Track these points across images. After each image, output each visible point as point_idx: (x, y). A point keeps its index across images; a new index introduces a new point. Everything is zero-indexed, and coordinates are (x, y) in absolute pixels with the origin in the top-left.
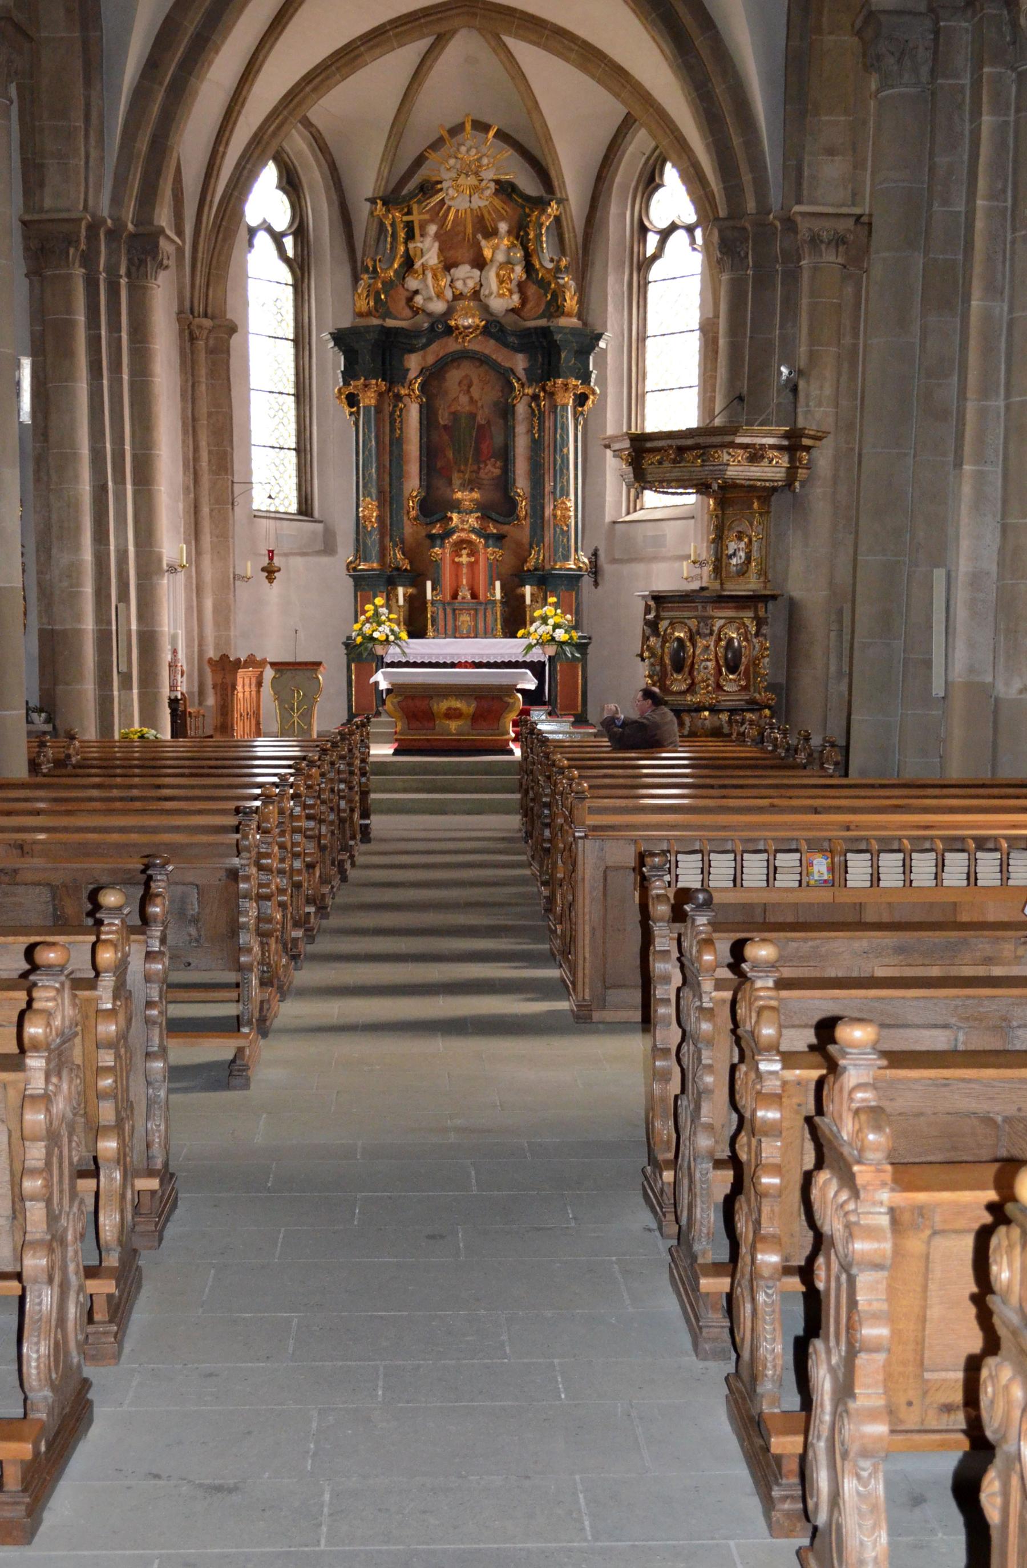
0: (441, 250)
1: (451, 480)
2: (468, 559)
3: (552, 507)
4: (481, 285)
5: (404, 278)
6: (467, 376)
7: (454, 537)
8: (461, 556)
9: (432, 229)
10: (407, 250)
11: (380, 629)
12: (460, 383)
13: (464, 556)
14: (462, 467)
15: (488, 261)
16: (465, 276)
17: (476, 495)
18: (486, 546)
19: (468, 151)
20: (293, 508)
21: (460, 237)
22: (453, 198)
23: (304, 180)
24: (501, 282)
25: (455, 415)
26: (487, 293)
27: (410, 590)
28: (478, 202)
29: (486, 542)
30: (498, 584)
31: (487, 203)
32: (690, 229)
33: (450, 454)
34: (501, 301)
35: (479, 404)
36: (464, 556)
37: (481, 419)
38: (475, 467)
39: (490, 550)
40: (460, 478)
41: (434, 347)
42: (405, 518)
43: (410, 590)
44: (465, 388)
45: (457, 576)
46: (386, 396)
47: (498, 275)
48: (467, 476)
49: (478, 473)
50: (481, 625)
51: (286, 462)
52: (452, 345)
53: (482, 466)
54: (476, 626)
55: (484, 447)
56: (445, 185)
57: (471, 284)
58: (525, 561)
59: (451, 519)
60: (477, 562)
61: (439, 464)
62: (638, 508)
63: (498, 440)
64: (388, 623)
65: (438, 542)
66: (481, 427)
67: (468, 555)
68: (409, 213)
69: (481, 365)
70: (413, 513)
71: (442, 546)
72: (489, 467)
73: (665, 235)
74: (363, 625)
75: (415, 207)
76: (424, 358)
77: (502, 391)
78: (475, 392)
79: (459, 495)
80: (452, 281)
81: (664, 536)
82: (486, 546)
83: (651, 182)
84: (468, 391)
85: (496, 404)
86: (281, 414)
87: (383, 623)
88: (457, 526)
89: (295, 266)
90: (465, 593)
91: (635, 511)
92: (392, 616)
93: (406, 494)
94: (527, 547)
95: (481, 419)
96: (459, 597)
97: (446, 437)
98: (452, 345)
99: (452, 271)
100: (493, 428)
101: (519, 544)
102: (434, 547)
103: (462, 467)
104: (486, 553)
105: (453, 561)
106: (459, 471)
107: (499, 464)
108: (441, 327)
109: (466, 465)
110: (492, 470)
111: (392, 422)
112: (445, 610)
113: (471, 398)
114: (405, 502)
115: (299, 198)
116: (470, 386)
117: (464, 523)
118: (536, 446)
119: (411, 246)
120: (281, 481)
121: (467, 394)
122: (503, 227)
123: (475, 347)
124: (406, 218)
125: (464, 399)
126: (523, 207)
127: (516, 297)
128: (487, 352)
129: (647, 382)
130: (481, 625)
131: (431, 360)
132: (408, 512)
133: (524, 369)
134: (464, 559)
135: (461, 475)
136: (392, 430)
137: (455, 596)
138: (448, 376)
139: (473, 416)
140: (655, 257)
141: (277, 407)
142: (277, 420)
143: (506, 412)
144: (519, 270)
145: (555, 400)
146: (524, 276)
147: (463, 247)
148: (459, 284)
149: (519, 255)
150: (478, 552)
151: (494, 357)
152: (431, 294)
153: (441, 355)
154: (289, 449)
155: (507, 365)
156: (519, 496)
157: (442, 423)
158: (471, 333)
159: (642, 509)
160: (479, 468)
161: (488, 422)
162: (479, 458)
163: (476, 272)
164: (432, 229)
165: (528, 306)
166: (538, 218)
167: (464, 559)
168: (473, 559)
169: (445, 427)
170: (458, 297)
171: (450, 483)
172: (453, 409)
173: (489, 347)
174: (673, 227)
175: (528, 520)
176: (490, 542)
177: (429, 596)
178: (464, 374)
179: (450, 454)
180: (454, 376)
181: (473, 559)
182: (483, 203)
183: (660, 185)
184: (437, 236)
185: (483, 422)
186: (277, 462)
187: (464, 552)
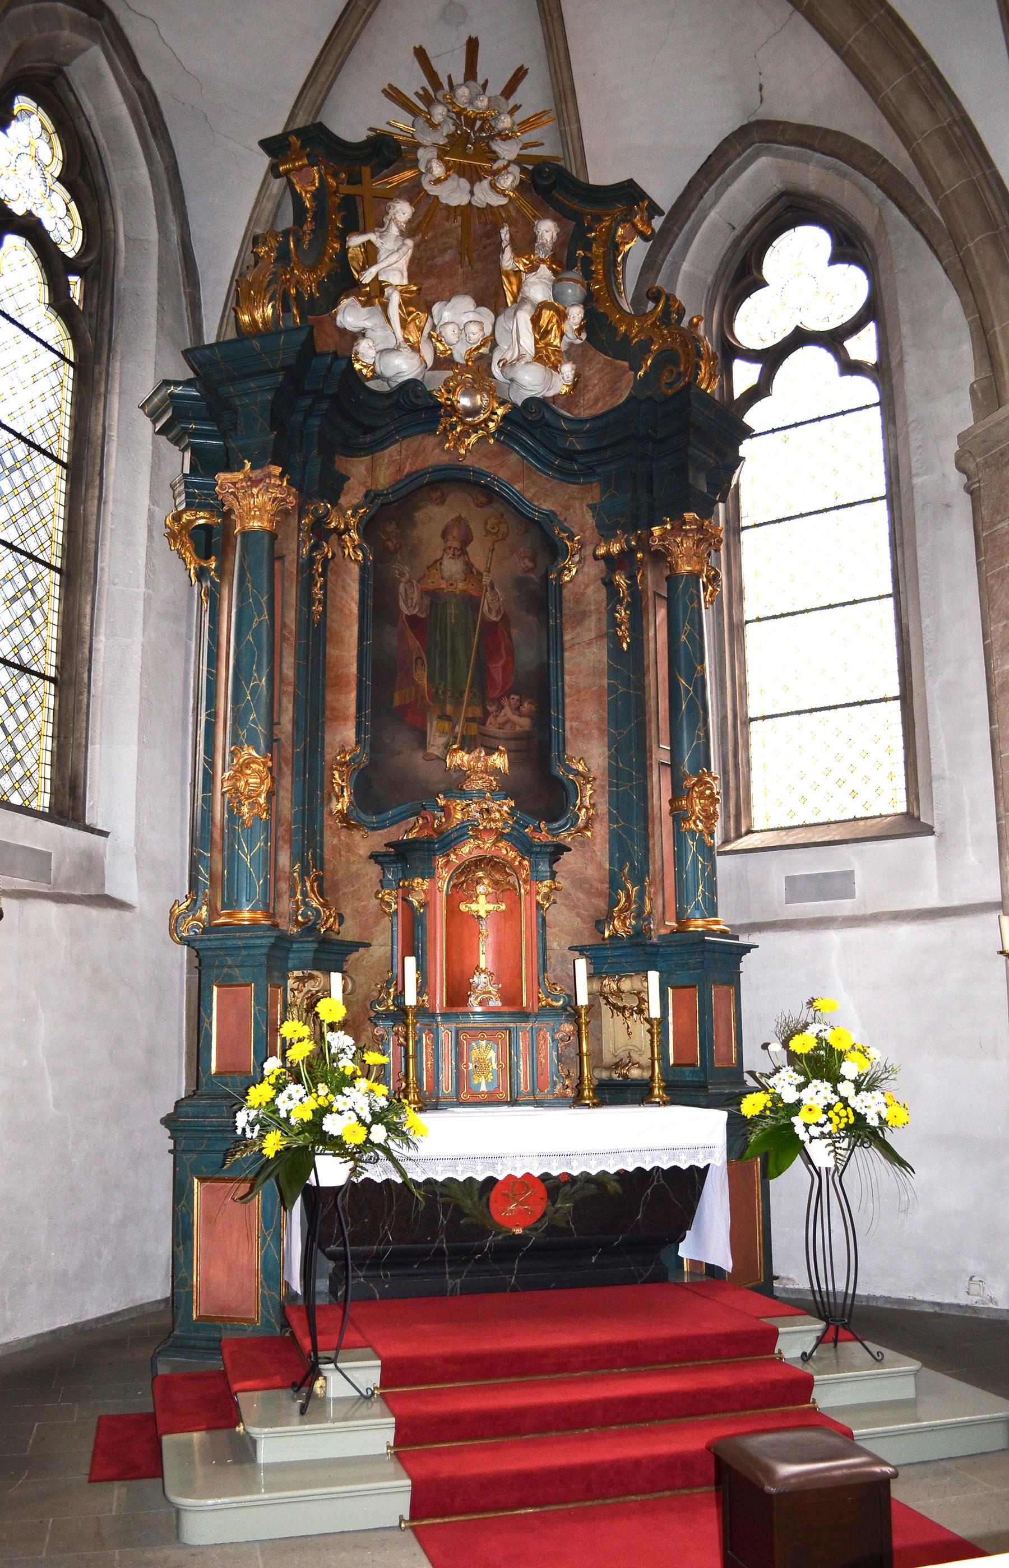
0: (416, 269)
1: (424, 734)
2: (491, 907)
3: (667, 795)
4: (494, 345)
5: (336, 304)
6: (459, 520)
7: (466, 850)
8: (472, 898)
9: (402, 211)
10: (345, 250)
11: (340, 1103)
12: (444, 535)
13: (482, 899)
14: (449, 709)
15: (509, 299)
16: (460, 322)
17: (500, 761)
19: (471, 102)
20: (43, 802)
21: (448, 257)
22: (438, 181)
23: (115, 177)
24: (542, 334)
25: (435, 598)
26: (508, 357)
28: (485, 196)
31: (504, 201)
32: (833, 340)
33: (422, 678)
34: (532, 381)
35: (486, 580)
36: (482, 899)
37: (489, 609)
38: (478, 712)
40: (443, 733)
41: (392, 451)
44: (456, 544)
46: (294, 521)
47: (535, 320)
48: (458, 729)
49: (483, 723)
51: (33, 702)
52: (429, 452)
53: (492, 708)
55: (497, 669)
56: (421, 153)
57: (475, 335)
58: (610, 918)
61: (397, 700)
62: (743, 830)
63: (527, 657)
64: (362, 1083)
66: (489, 629)
68: (355, 180)
69: (490, 502)
70: (341, 805)
72: (507, 711)
73: (771, 359)
74: (279, 1088)
75: (366, 171)
76: (372, 470)
77: (532, 559)
78: (477, 553)
80: (434, 327)
81: (849, 875)
83: (743, 277)
84: (462, 552)
85: (521, 583)
86: (28, 598)
87: (350, 1081)
89: (84, 326)
91: (739, 836)
92: (373, 1058)
93: (331, 753)
95: (489, 609)
97: (414, 643)
98: (429, 452)
99: (436, 309)
100: (514, 632)
103: (449, 709)
106: (443, 717)
107: (526, 706)
108: (413, 407)
109: (458, 704)
110: (514, 717)
111: (307, 583)
113: (469, 566)
115: (101, 212)
116: (466, 540)
118: (628, 665)
119: (355, 241)
120: (19, 742)
121: (455, 558)
122: (547, 230)
123: (482, 465)
124: (346, 189)
125: (452, 567)
126: (577, 217)
127: (568, 370)
128: (503, 474)
129: (746, 605)
130: (523, 1070)
131: (384, 479)
133: (592, 507)
135: (446, 725)
136: (307, 599)
138: (419, 515)
139: (472, 603)
140: (760, 391)
141: (21, 583)
142: (18, 608)
143: (543, 600)
144: (576, 314)
145: (672, 567)
146: (584, 336)
147: (461, 259)
148: (450, 333)
149: (573, 291)
151: (517, 487)
152: (385, 348)
153: (407, 469)
154: (42, 676)
155: (546, 506)
156: (577, 773)
157: (406, 611)
158: (475, 428)
159: (750, 832)
160: (486, 714)
161: (505, 618)
162: (485, 691)
163: (486, 315)
164: (402, 211)
165: (590, 396)
166: (612, 232)
167: (482, 906)
169: (412, 620)
170: (443, 362)
171: (422, 742)
172: (430, 584)
173: (509, 470)
174: (800, 338)
178: (453, 516)
179: (422, 678)
180: (434, 518)
182: (498, 201)
183: (761, 283)
184: (409, 231)
185: (493, 617)
186: (13, 697)
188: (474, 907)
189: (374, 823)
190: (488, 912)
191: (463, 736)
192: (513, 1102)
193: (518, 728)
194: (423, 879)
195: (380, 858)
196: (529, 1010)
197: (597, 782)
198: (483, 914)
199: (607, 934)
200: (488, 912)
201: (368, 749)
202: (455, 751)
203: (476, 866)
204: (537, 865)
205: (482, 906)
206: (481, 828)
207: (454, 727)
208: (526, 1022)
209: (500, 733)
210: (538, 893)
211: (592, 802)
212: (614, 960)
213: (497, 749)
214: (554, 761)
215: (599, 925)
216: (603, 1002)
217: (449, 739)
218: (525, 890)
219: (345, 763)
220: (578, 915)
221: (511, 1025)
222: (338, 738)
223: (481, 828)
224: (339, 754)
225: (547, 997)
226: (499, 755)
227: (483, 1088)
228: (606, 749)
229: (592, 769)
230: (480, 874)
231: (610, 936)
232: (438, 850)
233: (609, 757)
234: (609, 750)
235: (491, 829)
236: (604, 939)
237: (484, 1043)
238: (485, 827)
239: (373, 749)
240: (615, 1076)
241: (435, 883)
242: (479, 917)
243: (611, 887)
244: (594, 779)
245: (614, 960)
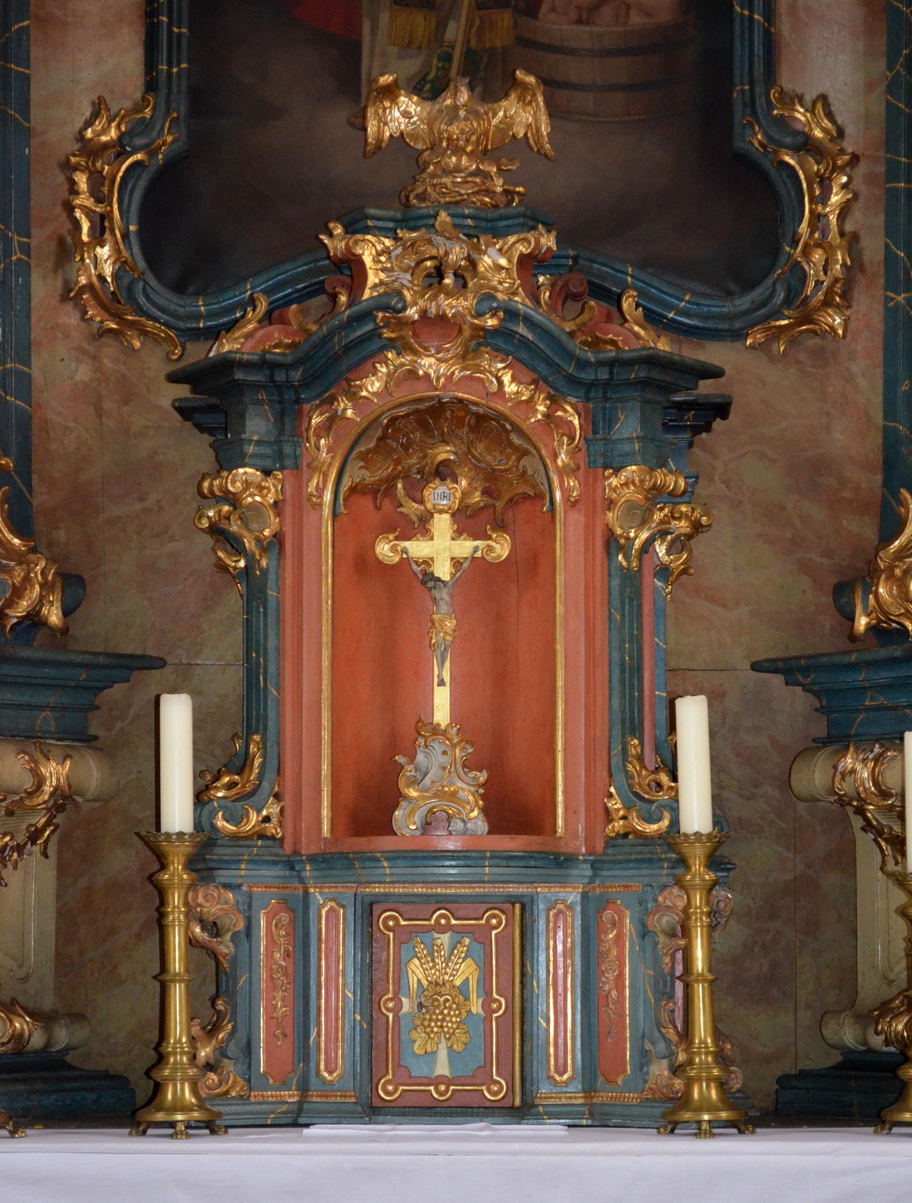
2: (465, 547)
7: (373, 385)
13: (442, 524)
17: (523, 115)
18: (601, 456)
27: (55, 772)
29: (598, 424)
30: (693, 717)
36: (442, 524)
39: (625, 482)
40: (409, 45)
42: (42, 288)
43: (55, 772)
45: (390, 674)
48: (454, 32)
50: (559, 1020)
54: (525, 1013)
58: (868, 575)
59: (352, 268)
60: (531, 565)
65: (257, 425)
67: (467, 522)
71: (281, 457)
79: (402, 115)
82: (601, 456)
88: (391, 302)
90: (441, 796)
94: (871, 482)
96: (407, 821)
101: (811, 471)
102: (227, 458)
104: (593, 503)
105: (364, 564)
112: (299, 913)
114: (44, 191)
117: (446, 291)
130: (559, 1020)
132: (67, 249)
134: (442, 549)
137: (371, 808)
150: (539, 496)
156: (805, 145)
168: (501, 548)
175: (869, 307)
176: (628, 426)
177: (178, 813)
181: (501, 548)
187: (440, 495)
188: (417, 548)
189: (198, 317)
190: (457, 563)
191: (470, 56)
192: (522, 1110)
193: (636, 19)
194: (267, 473)
195: (198, 417)
196: (567, 848)
197: (862, 169)
198: (443, 570)
199: (862, 622)
200: (457, 563)
201: (181, 107)
202: (390, 93)
203: (422, 424)
204: (610, 422)
205: (442, 549)
206: (412, 312)
207: (442, 27)
208: (563, 881)
209: (579, 35)
210: (610, 504)
211: (849, 227)
212: (881, 700)
213: (515, 83)
214: (739, 115)
215: (844, 592)
216: (857, 822)
217: (427, 64)
218: (566, 492)
219: (106, 146)
220: (805, 568)
221: (523, 889)
222: (88, 74)
223: (412, 312)
224: (89, 123)
225: (628, 807)
226: (521, 99)
227: (442, 1068)
228: (882, 63)
229: (849, 130)
230: (444, 453)
231: (870, 628)
232: (306, 383)
233: (890, 90)
234: (890, 68)
235: (442, 318)
236: (853, 637)
237: (445, 939)
238: (424, 313)
239: (203, 101)
240: (877, 1041)
241: (300, 486)
242: (429, 579)
243: (885, 484)
244: (855, 159)
245: (881, 700)
